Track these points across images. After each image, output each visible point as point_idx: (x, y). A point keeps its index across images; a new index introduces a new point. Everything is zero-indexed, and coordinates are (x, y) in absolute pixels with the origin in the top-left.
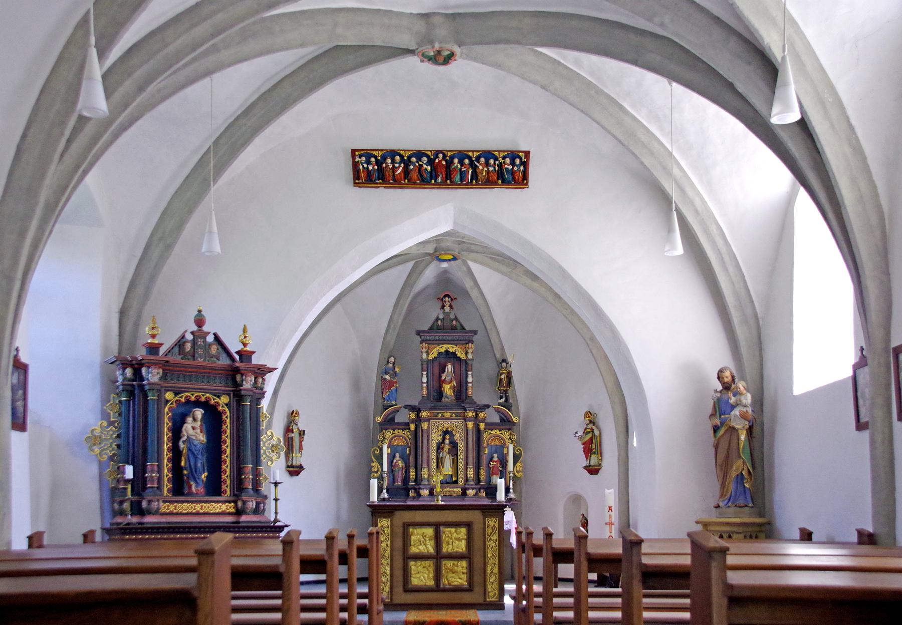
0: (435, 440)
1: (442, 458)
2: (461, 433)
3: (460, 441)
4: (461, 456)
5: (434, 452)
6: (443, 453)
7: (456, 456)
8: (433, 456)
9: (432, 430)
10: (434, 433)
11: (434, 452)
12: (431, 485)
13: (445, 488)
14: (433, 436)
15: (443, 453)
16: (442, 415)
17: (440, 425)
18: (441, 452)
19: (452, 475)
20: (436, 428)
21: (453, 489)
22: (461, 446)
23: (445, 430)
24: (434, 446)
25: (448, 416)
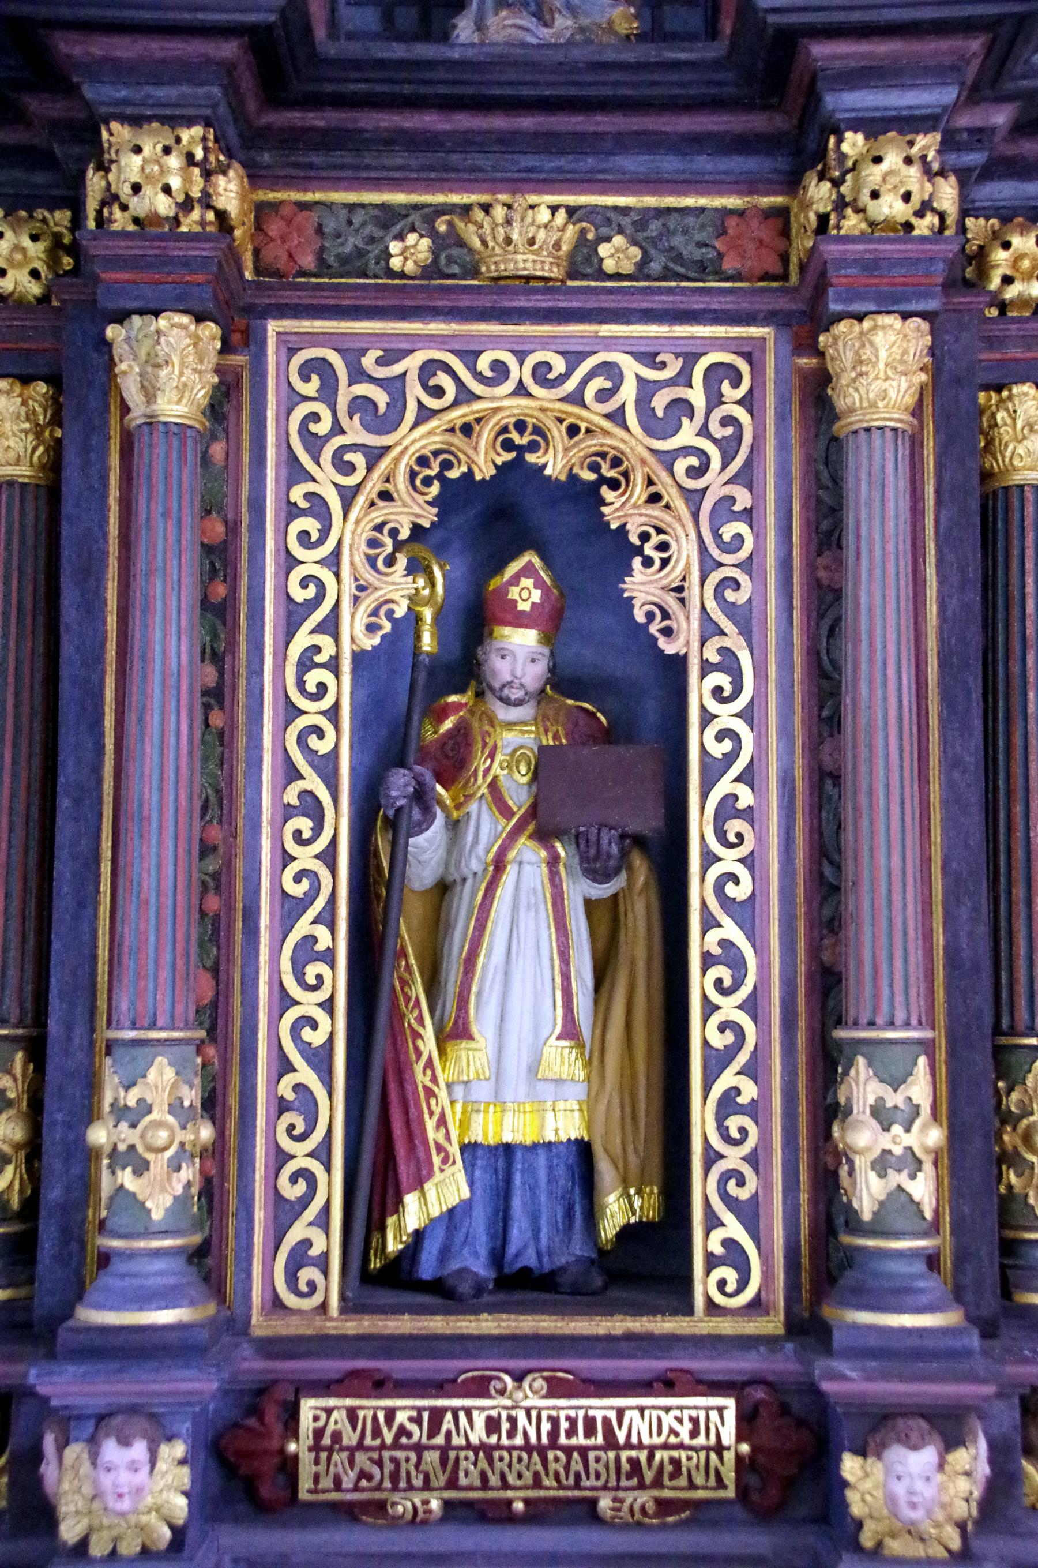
0: (331, 626)
1: (443, 889)
2: (725, 507)
3: (710, 630)
4: (729, 861)
5: (310, 805)
6: (455, 827)
7: (640, 865)
8: (305, 858)
9: (295, 472)
10: (318, 506)
11: (310, 805)
12: (260, 1324)
13: (480, 1388)
14: (310, 560)
15: (455, 827)
16: (441, 243)
17: (415, 391)
18: (421, 797)
19: (583, 1150)
20: (356, 433)
21: (601, 1407)
22: (726, 715)
23: (484, 471)
24: (313, 712)
25: (525, 263)
